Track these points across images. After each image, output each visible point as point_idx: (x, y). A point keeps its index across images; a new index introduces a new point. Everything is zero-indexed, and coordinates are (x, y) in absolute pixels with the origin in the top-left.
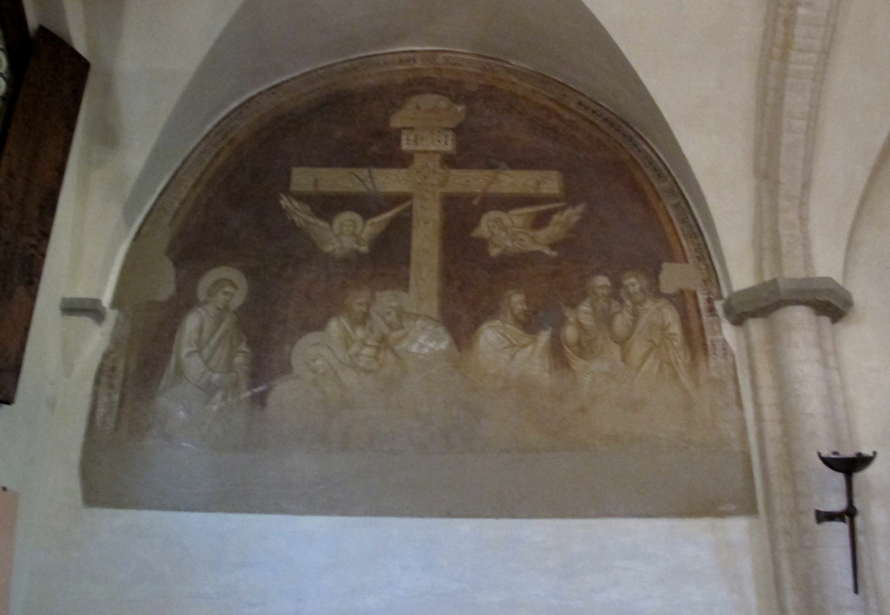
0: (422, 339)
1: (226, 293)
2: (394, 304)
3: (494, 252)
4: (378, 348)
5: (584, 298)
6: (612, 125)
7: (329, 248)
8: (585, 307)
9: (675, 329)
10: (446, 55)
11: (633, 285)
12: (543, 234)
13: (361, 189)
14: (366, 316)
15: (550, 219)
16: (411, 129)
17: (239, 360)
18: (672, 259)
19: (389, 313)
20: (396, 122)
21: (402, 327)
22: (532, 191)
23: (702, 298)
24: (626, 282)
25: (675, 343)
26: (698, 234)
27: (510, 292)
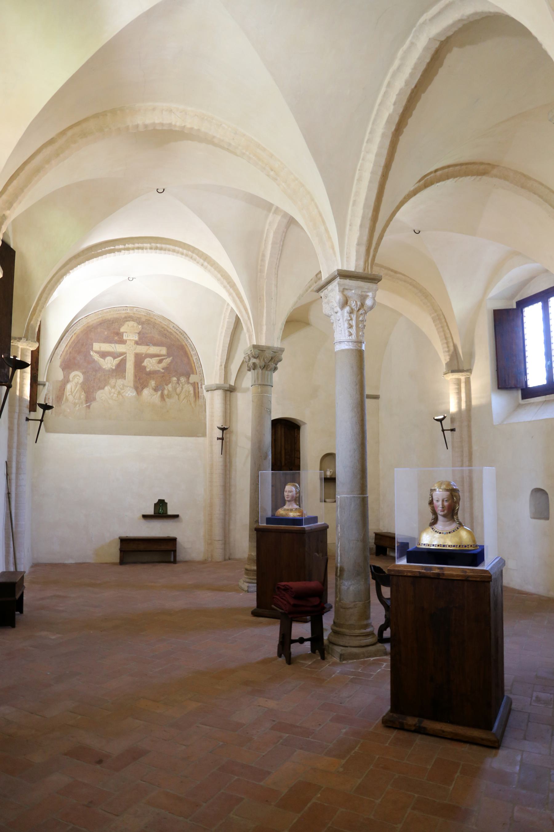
0: (129, 392)
1: (78, 379)
2: (122, 383)
3: (148, 370)
4: (118, 395)
6: (181, 334)
7: (104, 367)
8: (170, 386)
9: (192, 392)
10: (136, 308)
11: (183, 380)
13: (113, 350)
14: (115, 386)
16: (126, 332)
17: (82, 397)
18: (193, 373)
19: (121, 386)
20: (122, 330)
21: (124, 389)
23: (199, 385)
24: (181, 379)
26: (201, 367)
27: (151, 381)
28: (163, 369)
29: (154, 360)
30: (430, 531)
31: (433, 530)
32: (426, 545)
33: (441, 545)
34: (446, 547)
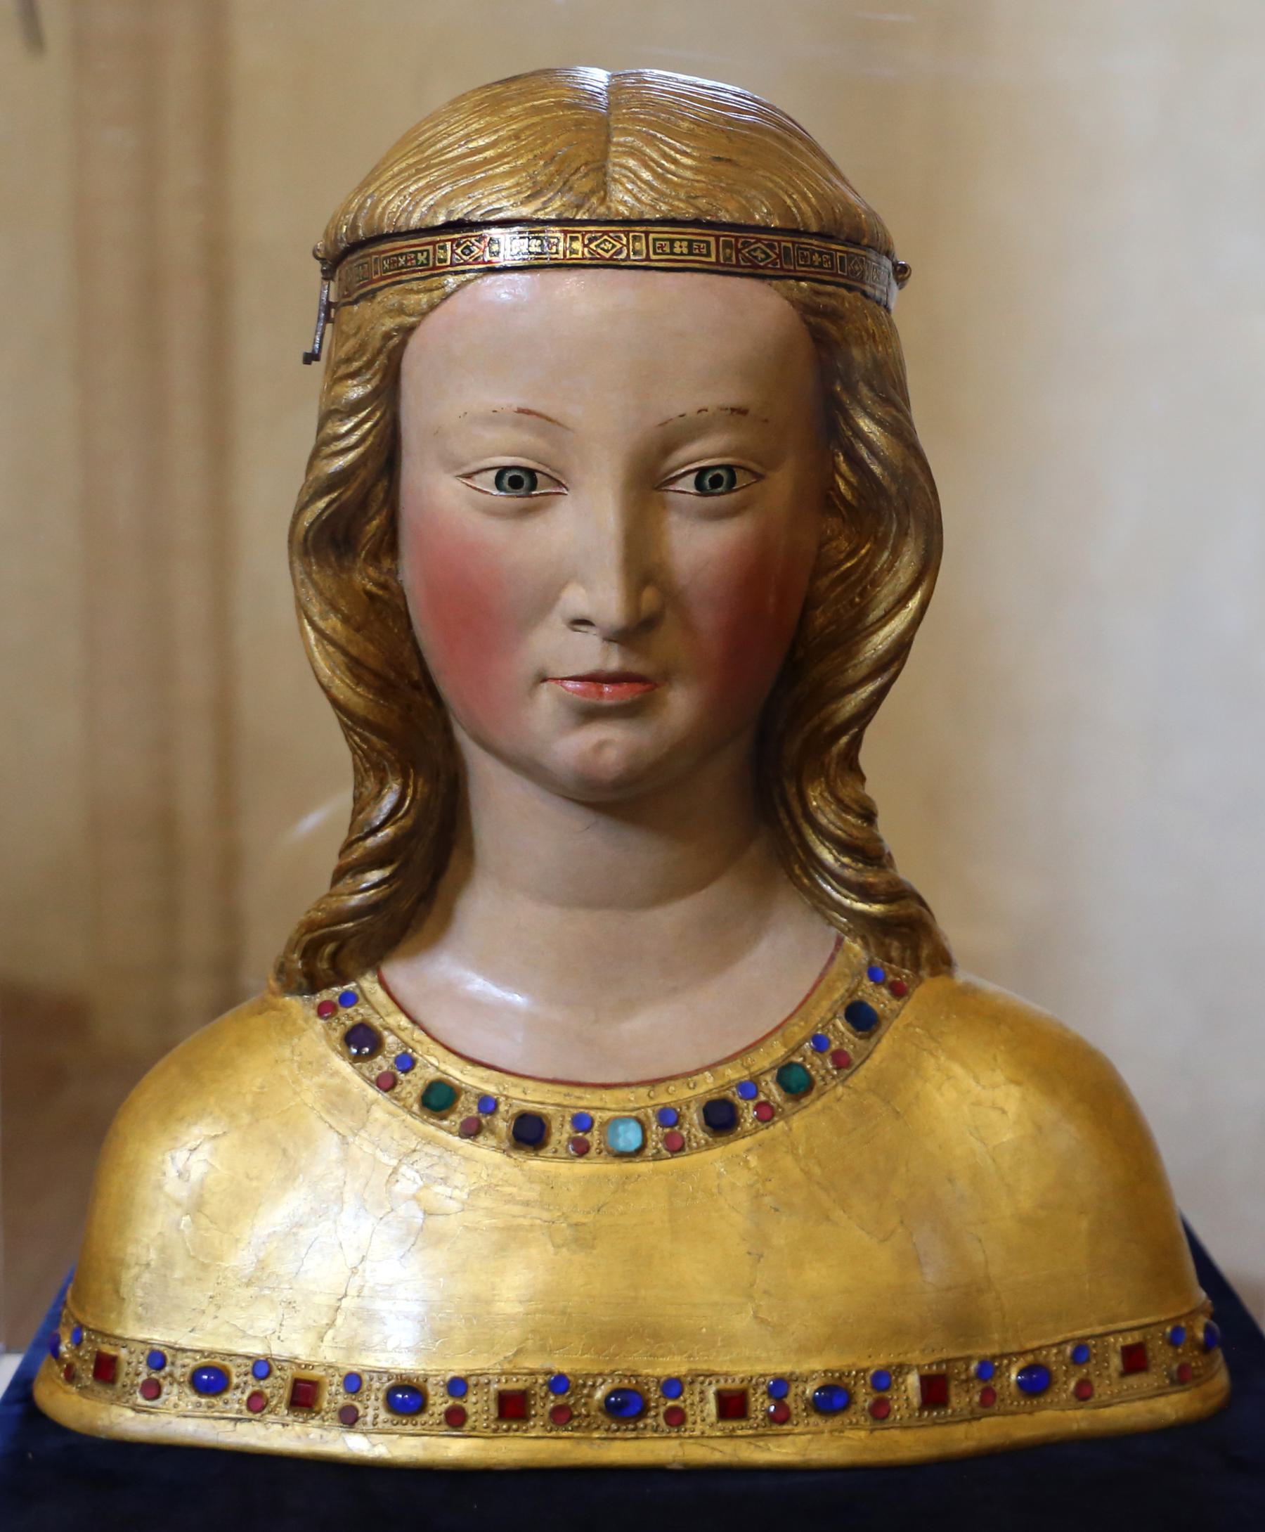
30: (309, 1091)
31: (383, 1063)
32: (235, 1399)
33: (559, 1383)
34: (676, 1418)
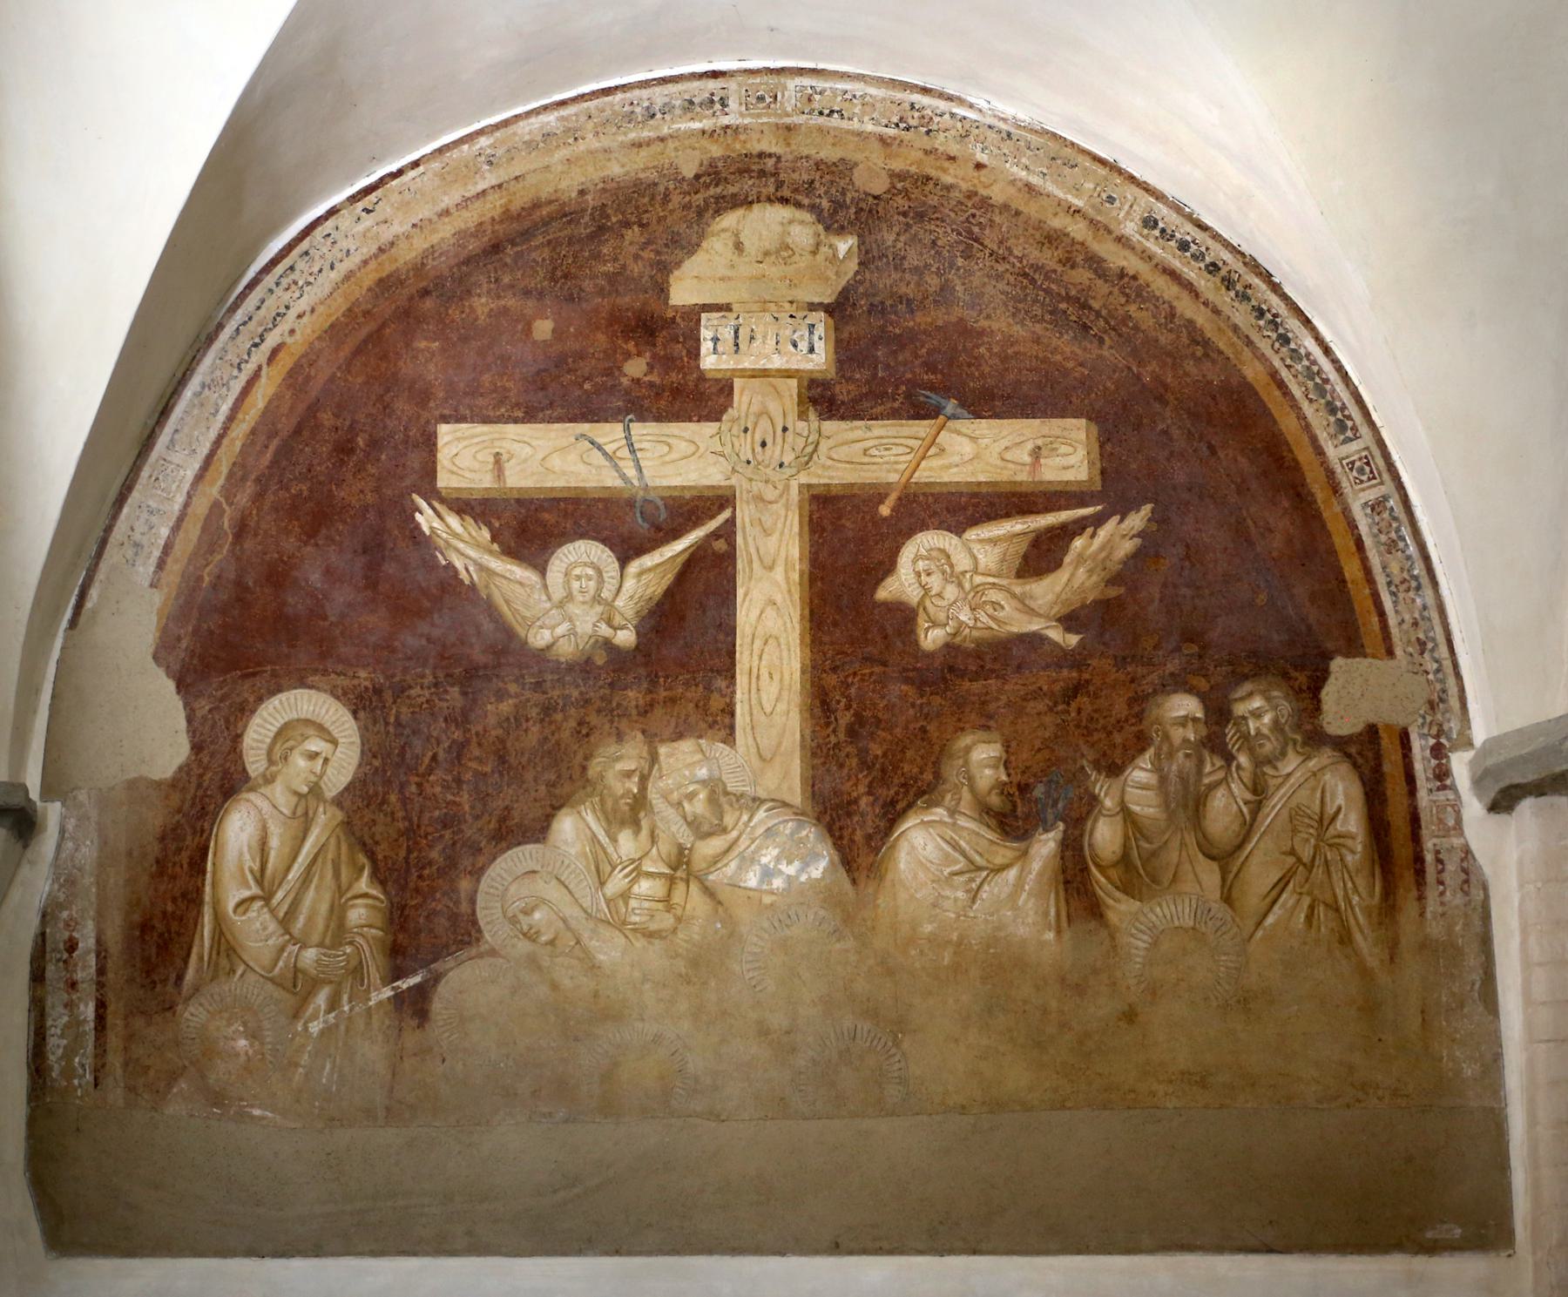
0: (768, 857)
1: (313, 756)
2: (703, 773)
3: (931, 638)
4: (671, 881)
5: (1142, 750)
6: (1228, 283)
7: (540, 638)
8: (1141, 773)
9: (1352, 823)
10: (807, 81)
11: (1257, 714)
12: (1049, 590)
13: (611, 480)
14: (640, 802)
15: (1065, 550)
16: (727, 308)
17: (357, 914)
18: (1353, 646)
19: (691, 797)
20: (683, 292)
22: (1023, 476)
24: (1240, 709)
25: (1349, 858)
26: (1425, 581)
27: (966, 740)
28: (1069, 621)
29: (981, 541)
